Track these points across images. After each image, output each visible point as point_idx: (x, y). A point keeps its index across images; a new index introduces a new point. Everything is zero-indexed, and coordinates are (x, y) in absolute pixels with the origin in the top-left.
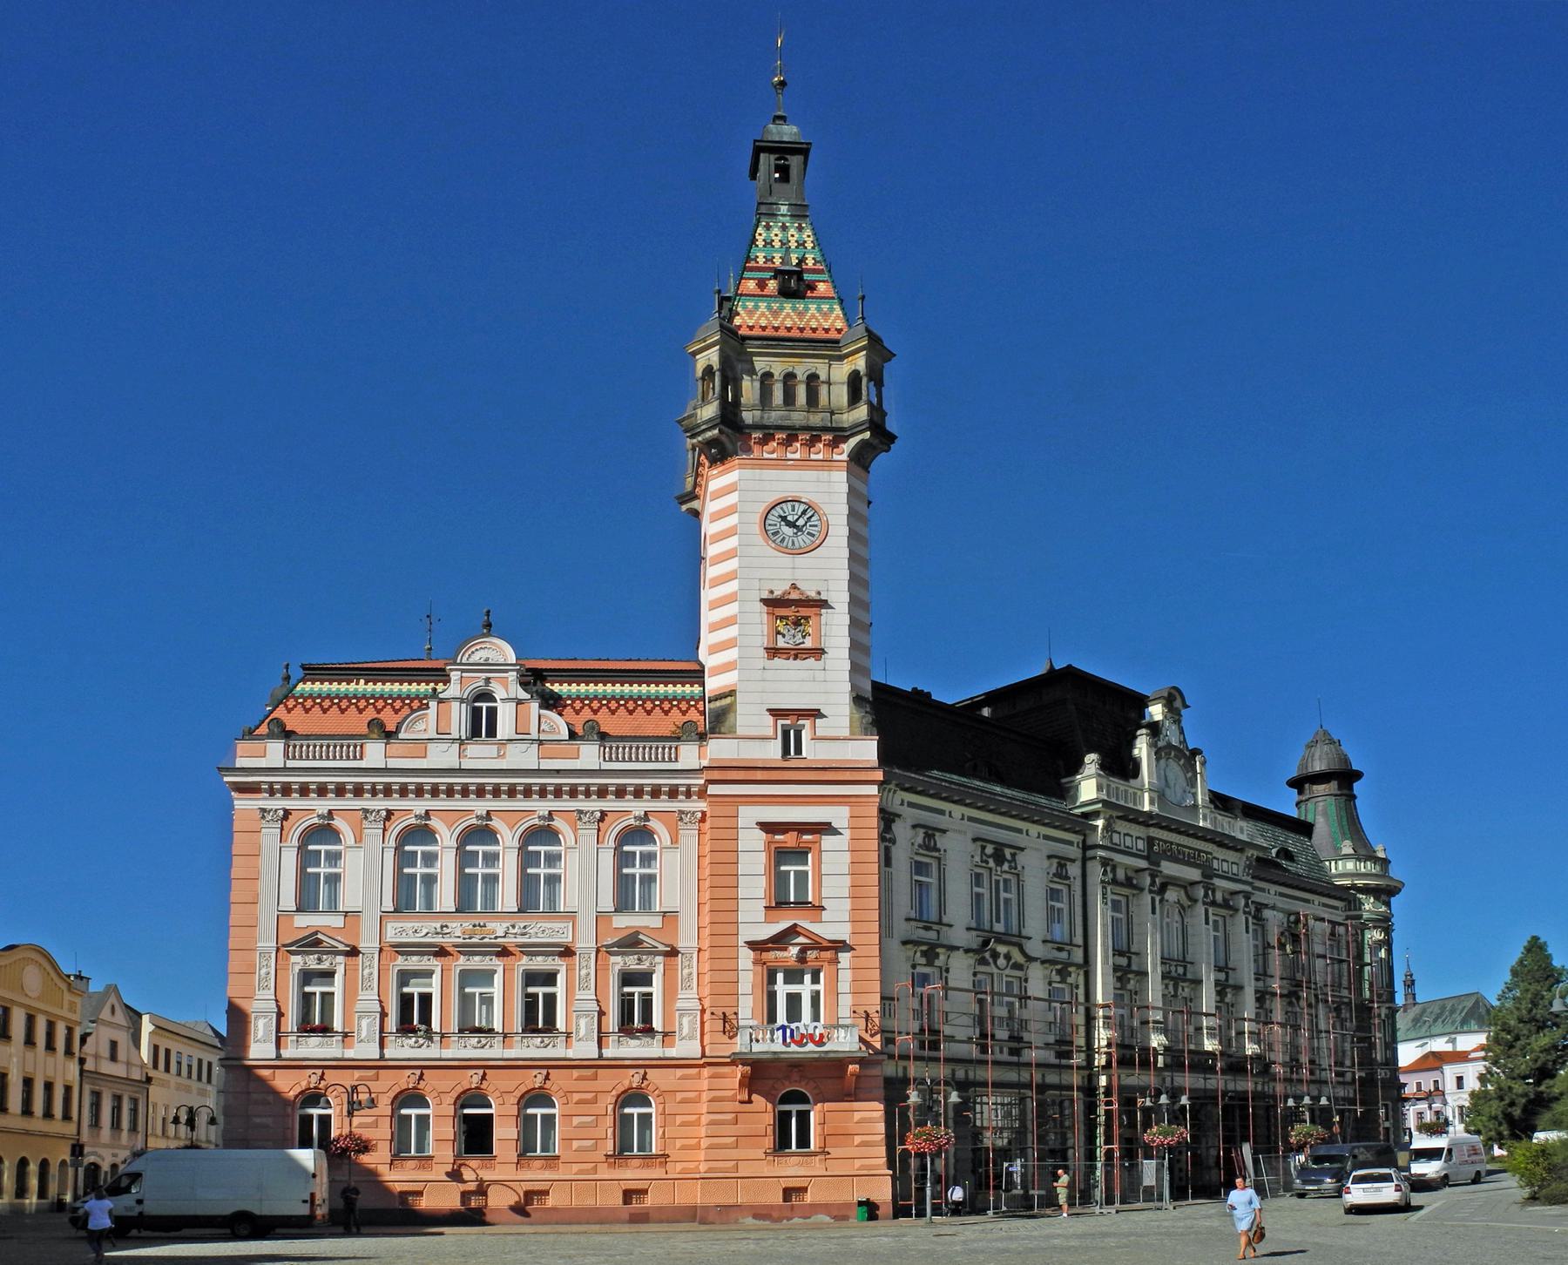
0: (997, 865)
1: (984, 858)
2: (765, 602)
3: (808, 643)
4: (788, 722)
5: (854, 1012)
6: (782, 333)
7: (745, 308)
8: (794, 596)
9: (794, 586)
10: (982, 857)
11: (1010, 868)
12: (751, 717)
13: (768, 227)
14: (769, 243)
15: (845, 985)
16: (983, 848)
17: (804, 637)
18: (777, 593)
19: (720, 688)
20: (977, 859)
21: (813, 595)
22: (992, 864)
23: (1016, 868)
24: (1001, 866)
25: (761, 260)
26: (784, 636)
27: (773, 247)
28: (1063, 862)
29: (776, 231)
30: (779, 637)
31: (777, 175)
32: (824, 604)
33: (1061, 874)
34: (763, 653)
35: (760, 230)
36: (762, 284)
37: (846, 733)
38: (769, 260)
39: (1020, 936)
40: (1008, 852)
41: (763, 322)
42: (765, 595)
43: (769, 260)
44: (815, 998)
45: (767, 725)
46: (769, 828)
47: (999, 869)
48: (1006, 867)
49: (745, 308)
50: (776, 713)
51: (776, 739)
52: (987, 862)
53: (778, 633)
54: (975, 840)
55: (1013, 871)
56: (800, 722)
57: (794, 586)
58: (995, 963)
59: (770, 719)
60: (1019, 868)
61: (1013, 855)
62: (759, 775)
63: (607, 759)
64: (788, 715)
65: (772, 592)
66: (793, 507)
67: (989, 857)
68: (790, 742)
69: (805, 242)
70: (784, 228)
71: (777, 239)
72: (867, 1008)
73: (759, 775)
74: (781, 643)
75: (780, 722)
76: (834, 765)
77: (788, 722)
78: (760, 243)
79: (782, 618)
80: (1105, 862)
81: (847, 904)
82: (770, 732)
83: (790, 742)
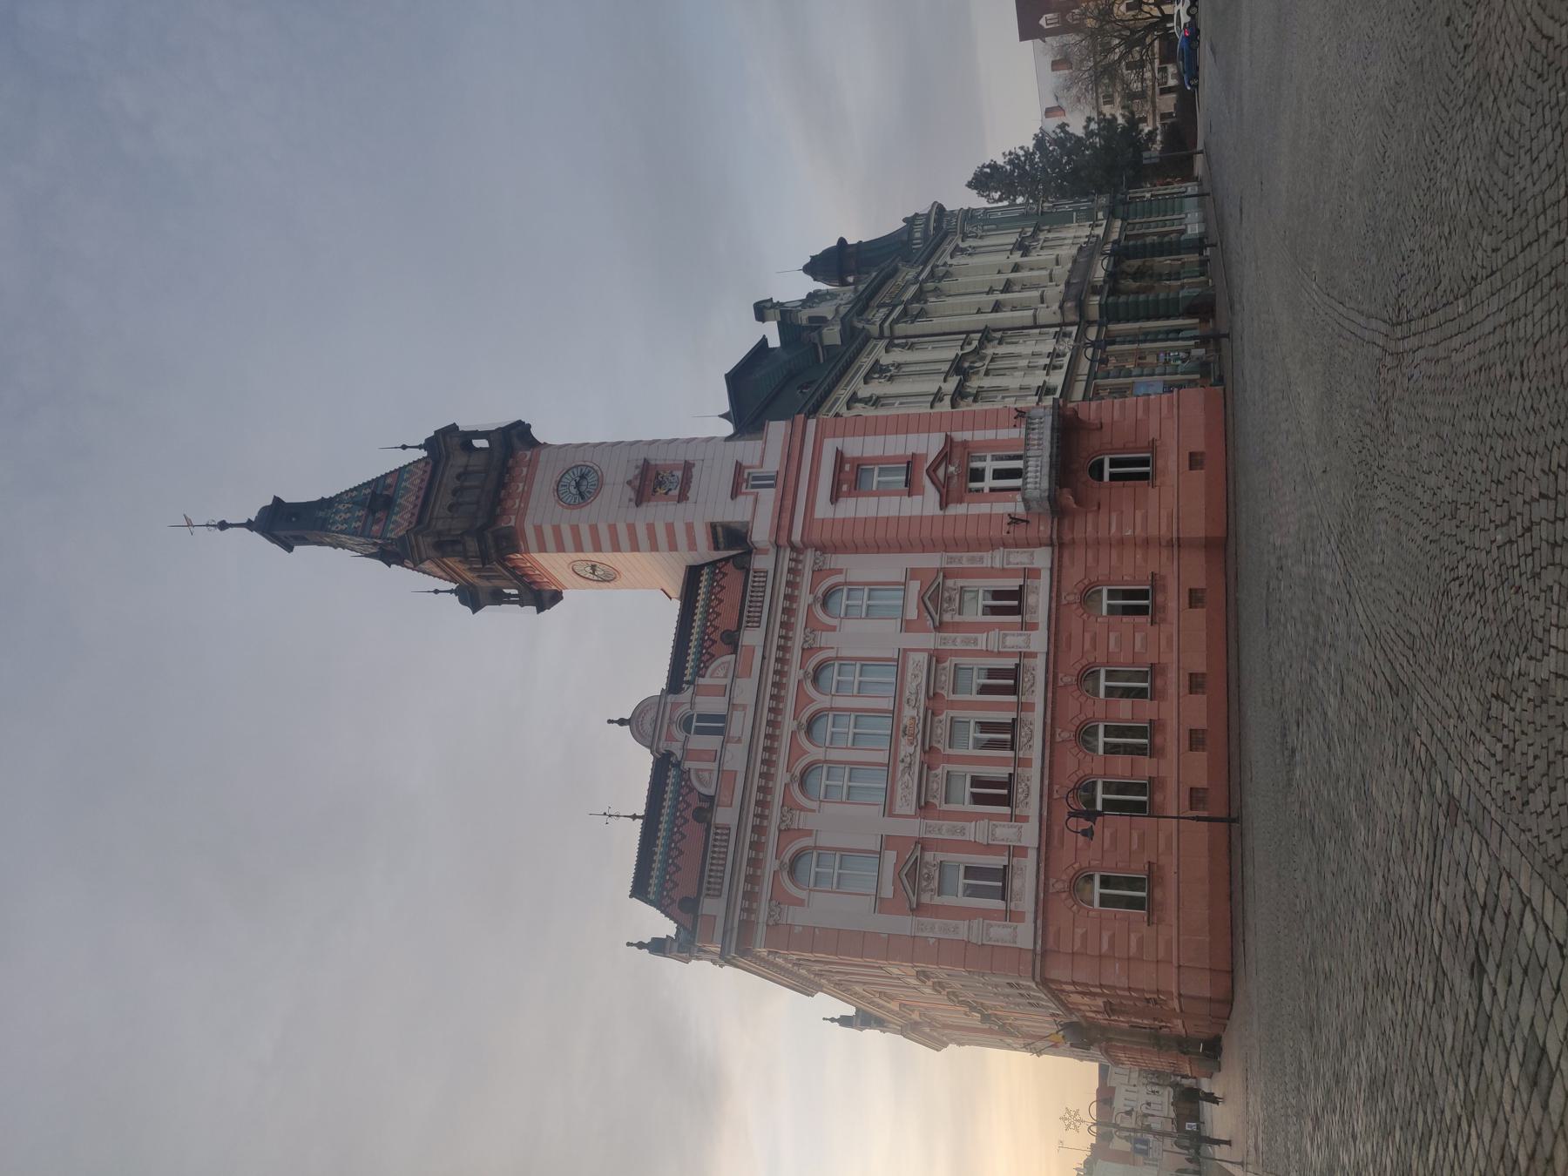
2: (638, 503)
3: (679, 474)
4: (744, 485)
5: (1015, 426)
6: (419, 502)
7: (393, 530)
8: (637, 483)
9: (629, 483)
12: (734, 512)
13: (334, 523)
14: (345, 521)
15: (990, 435)
17: (673, 476)
18: (633, 495)
19: (707, 533)
21: (637, 472)
22: (889, 374)
25: (359, 524)
26: (670, 490)
27: (349, 518)
29: (337, 518)
30: (670, 493)
31: (294, 519)
32: (646, 461)
33: (902, 346)
34: (681, 506)
35: (333, 529)
36: (377, 521)
37: (759, 443)
38: (359, 519)
39: (953, 361)
41: (407, 516)
42: (633, 504)
43: (359, 519)
44: (996, 458)
45: (745, 501)
46: (835, 497)
49: (393, 530)
50: (735, 493)
51: (758, 493)
53: (666, 493)
54: (866, 383)
56: (746, 476)
57: (629, 483)
59: (741, 498)
61: (882, 365)
62: (788, 503)
63: (757, 625)
64: (738, 484)
65: (630, 500)
66: (562, 486)
68: (763, 481)
69: (351, 497)
70: (335, 513)
71: (344, 516)
72: (1012, 417)
73: (788, 503)
74: (675, 492)
75: (744, 490)
76: (787, 450)
77: (744, 485)
78: (345, 526)
79: (655, 491)
80: (896, 321)
81: (912, 437)
82: (751, 498)
83: (763, 481)
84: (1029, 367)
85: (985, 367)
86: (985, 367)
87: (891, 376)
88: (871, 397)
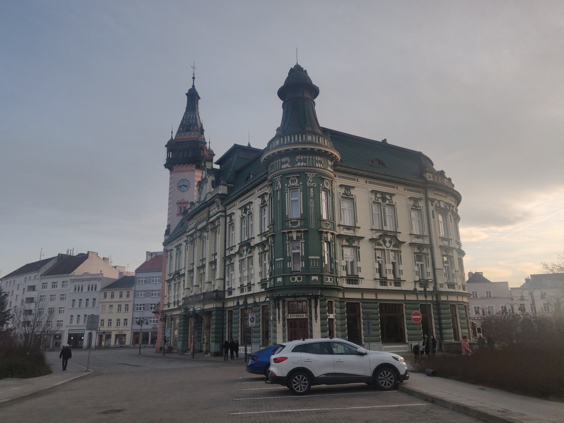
0: (383, 202)
1: (377, 199)
10: (375, 198)
11: (390, 202)
16: (376, 195)
20: (374, 199)
22: (380, 201)
23: (392, 203)
24: (385, 202)
28: (416, 200)
40: (388, 197)
47: (384, 203)
48: (387, 202)
52: (378, 200)
55: (391, 204)
58: (385, 244)
60: (394, 203)
67: (379, 198)
84: (386, 269)
85: (385, 248)
86: (385, 248)
87: (380, 203)
88: (352, 195)
